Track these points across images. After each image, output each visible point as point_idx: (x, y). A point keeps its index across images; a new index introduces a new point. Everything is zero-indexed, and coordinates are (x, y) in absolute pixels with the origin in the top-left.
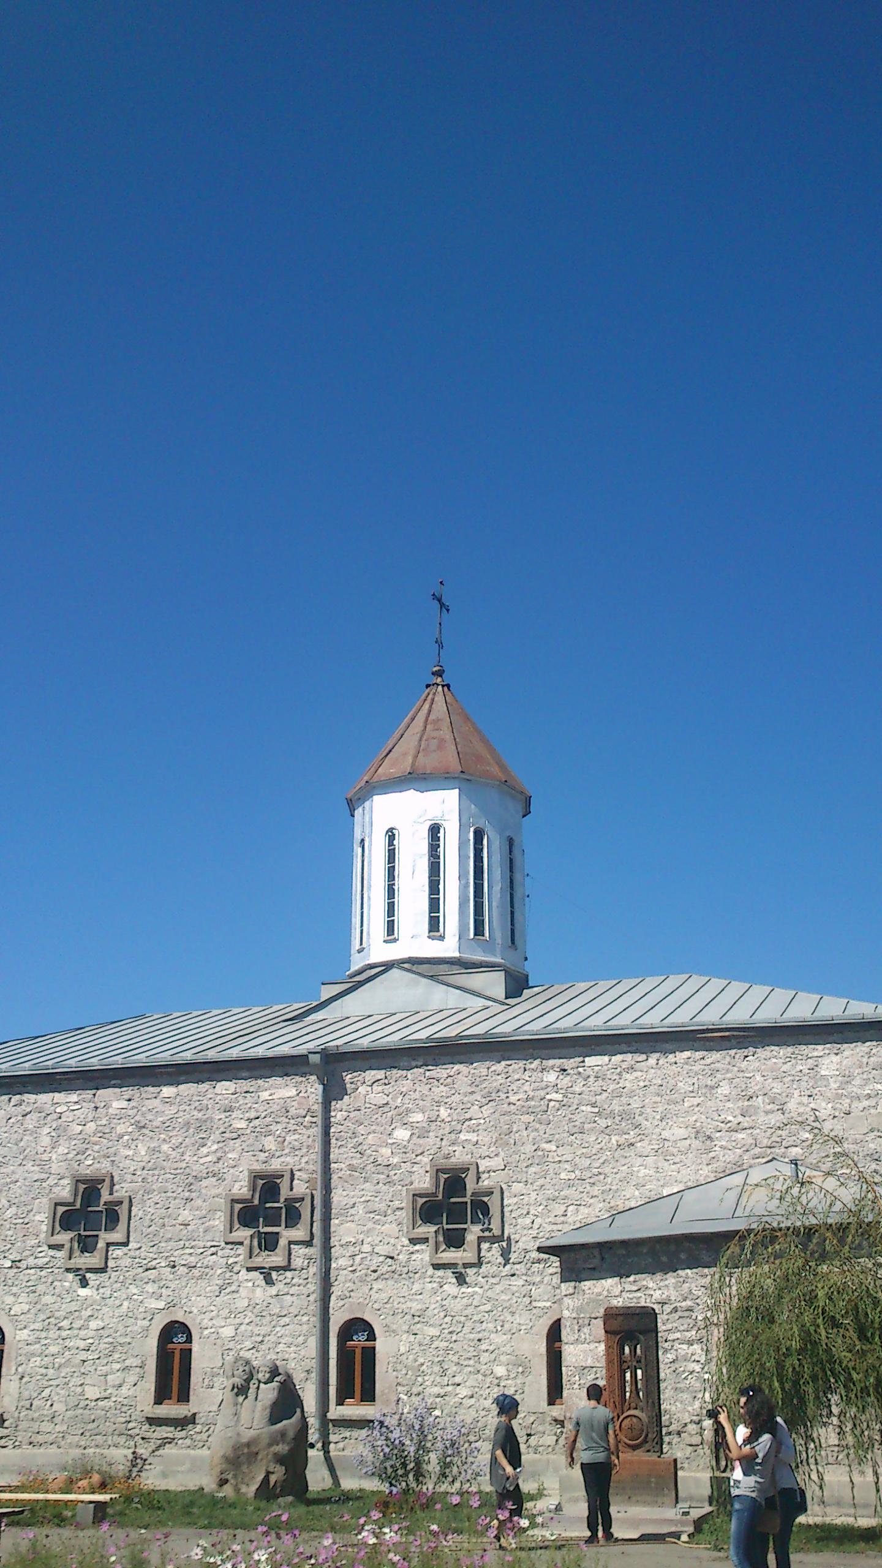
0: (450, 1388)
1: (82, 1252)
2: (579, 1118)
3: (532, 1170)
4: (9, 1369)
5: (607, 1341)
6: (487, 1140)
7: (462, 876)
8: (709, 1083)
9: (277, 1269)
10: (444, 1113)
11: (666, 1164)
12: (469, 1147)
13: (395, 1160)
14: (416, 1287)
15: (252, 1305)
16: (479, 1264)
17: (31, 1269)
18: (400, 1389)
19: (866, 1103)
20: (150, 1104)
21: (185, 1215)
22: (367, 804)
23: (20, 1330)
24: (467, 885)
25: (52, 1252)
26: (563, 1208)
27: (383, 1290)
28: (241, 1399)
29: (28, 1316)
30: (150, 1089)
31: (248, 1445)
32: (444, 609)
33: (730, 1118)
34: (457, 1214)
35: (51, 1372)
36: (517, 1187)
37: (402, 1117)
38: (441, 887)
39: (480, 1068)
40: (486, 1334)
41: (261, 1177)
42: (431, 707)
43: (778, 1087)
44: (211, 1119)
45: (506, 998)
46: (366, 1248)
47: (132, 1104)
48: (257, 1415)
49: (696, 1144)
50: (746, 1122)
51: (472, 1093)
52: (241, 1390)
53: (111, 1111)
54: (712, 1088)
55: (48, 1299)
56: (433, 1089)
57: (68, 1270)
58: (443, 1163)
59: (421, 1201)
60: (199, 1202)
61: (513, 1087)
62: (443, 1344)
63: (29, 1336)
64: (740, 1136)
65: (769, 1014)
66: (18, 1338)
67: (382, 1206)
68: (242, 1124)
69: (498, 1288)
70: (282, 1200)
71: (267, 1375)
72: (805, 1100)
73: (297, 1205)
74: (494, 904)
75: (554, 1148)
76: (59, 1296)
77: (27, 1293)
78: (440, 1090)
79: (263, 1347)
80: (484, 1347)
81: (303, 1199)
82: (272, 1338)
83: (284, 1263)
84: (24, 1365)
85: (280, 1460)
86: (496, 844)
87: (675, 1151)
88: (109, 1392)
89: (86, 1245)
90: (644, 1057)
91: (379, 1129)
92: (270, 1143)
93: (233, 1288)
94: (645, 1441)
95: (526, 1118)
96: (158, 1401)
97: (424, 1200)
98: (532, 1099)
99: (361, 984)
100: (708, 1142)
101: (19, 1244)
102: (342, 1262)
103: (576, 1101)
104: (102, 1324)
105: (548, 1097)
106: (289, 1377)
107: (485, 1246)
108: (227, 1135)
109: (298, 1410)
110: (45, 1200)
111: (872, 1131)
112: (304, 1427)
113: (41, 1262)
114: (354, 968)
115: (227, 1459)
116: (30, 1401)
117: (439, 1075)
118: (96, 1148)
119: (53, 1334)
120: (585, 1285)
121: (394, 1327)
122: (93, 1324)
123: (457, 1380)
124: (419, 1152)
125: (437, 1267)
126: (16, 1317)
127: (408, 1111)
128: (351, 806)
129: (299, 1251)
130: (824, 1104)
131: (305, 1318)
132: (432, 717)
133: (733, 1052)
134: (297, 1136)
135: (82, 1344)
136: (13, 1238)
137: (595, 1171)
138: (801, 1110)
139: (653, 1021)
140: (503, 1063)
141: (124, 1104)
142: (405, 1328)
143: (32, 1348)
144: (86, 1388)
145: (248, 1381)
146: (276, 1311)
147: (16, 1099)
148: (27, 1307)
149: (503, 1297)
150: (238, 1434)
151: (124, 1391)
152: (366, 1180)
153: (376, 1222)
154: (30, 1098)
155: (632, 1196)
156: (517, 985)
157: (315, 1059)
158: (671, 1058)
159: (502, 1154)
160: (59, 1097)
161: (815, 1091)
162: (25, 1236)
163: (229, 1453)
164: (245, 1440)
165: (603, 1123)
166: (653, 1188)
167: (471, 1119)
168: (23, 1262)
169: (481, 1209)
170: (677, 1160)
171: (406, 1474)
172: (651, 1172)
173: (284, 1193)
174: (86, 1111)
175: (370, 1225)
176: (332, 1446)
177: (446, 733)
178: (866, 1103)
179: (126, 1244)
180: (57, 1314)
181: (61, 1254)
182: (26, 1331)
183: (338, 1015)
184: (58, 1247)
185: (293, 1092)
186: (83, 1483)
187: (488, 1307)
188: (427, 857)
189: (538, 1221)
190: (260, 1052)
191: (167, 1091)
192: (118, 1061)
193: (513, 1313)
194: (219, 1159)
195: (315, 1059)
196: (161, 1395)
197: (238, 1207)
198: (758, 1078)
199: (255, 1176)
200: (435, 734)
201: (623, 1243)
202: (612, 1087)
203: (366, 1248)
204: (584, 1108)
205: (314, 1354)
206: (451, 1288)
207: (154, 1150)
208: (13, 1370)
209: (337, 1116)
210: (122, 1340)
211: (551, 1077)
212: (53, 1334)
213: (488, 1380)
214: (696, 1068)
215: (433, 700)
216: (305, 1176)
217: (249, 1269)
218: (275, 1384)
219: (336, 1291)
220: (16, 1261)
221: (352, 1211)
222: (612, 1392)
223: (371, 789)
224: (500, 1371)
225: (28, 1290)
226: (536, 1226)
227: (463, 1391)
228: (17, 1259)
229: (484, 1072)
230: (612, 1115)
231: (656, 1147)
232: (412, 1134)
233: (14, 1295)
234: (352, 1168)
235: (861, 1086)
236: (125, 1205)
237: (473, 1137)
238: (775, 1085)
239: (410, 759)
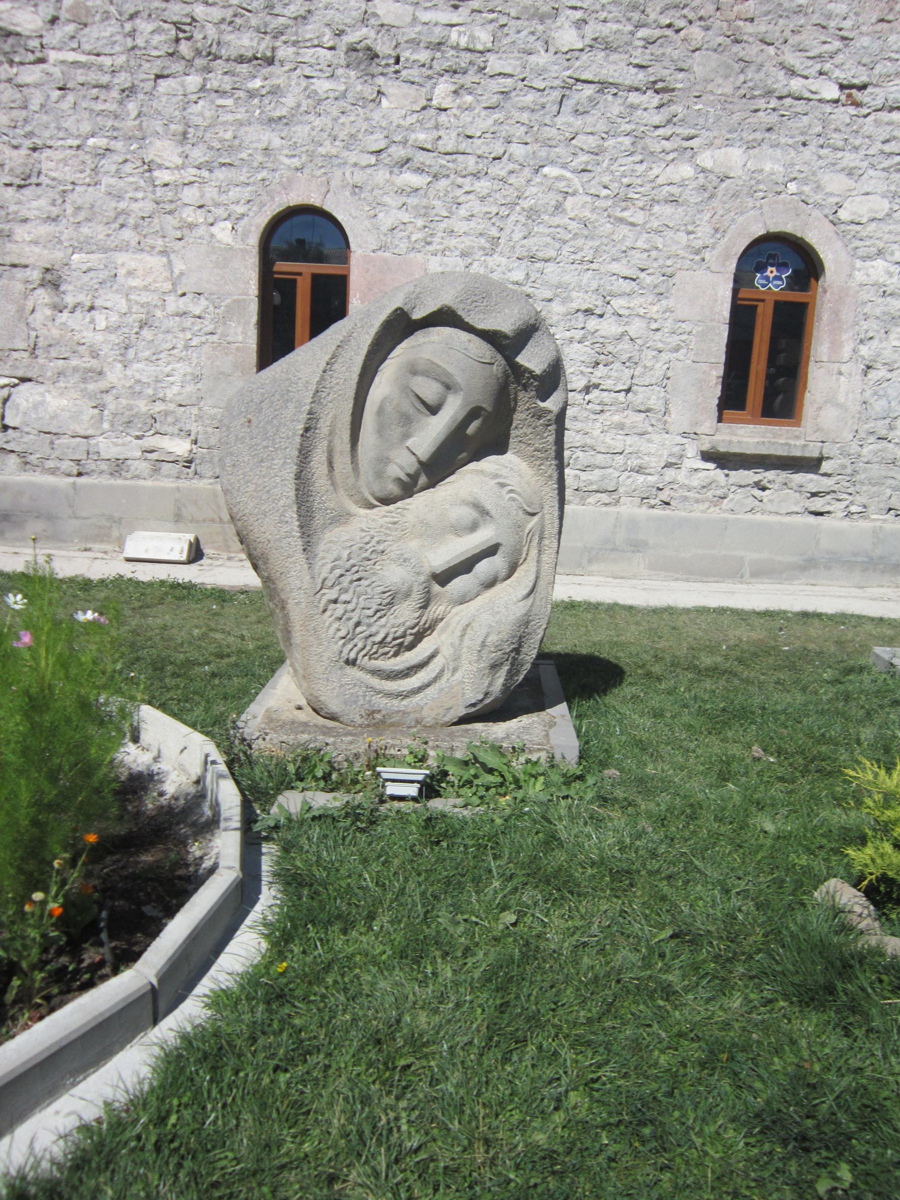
4: (836, 346)
17: (891, 109)
23: (864, 259)
29: (887, 228)
63: (890, 274)
66: (859, 277)
77: (884, 170)
84: (875, 343)
101: (865, 41)
116: (887, 421)
126: (858, 228)
136: (847, 24)
148: (884, 206)
162: (882, 20)
168: (870, 89)
182: (880, 263)
208: (846, 352)
220: (851, 87)
225: (886, 164)
228: (856, 81)
233: (850, 173)
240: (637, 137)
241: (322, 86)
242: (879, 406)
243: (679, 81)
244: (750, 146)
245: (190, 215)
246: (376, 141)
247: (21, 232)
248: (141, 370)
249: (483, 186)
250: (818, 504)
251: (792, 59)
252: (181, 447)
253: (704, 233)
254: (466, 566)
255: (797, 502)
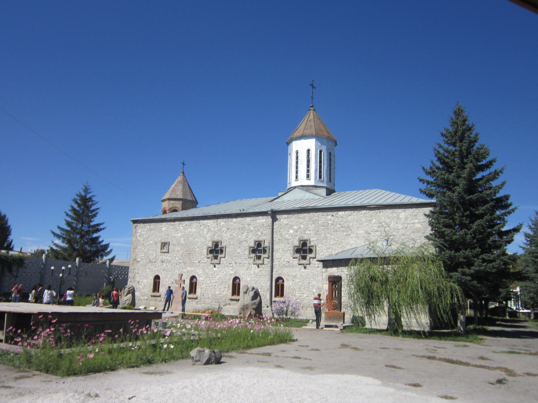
0: (302, 294)
1: (214, 259)
2: (336, 228)
3: (324, 241)
4: (198, 286)
5: (329, 283)
6: (313, 233)
7: (316, 163)
8: (370, 219)
9: (261, 264)
10: (302, 226)
11: (358, 240)
12: (308, 235)
13: (290, 238)
14: (294, 269)
15: (255, 273)
16: (310, 264)
18: (290, 294)
19: (411, 225)
20: (230, 223)
21: (239, 251)
22: (291, 144)
24: (317, 166)
25: (207, 259)
26: (331, 251)
27: (286, 270)
28: (245, 295)
30: (230, 219)
31: (246, 305)
32: (314, 88)
33: (375, 228)
34: (305, 251)
35: (208, 288)
36: (320, 245)
37: (291, 227)
38: (310, 166)
39: (311, 214)
40: (311, 281)
41: (257, 242)
42: (309, 116)
43: (388, 221)
44: (245, 227)
45: (326, 195)
46: (282, 260)
47: (226, 223)
48: (249, 298)
49: (366, 235)
50: (379, 229)
51: (309, 221)
52: (246, 293)
53: (221, 225)
54: (371, 220)
55: (207, 271)
56: (300, 220)
57: (211, 264)
58: (301, 239)
59: (296, 248)
60: (242, 247)
61: (320, 220)
62: (300, 284)
64: (378, 233)
65: (398, 201)
67: (287, 249)
68: (252, 228)
69: (314, 270)
70: (262, 247)
71: (251, 290)
72: (395, 224)
73: (266, 249)
74: (324, 171)
75: (329, 235)
76: (209, 270)
78: (301, 220)
79: (257, 283)
80: (310, 284)
81: (267, 247)
82: (259, 281)
83: (262, 263)
85: (254, 309)
86: (326, 154)
87: (360, 237)
88: (221, 292)
89: (216, 258)
90: (353, 212)
91: (286, 230)
92: (259, 233)
93: (250, 269)
94: (337, 308)
95: (322, 228)
96: (233, 295)
97: (297, 248)
98: (324, 223)
99: (287, 192)
100: (369, 235)
102: (276, 263)
103: (335, 224)
104: (219, 277)
105: (328, 222)
106: (258, 290)
107: (311, 260)
108: (249, 231)
109: (259, 298)
110: (206, 247)
111: (413, 232)
112: (260, 303)
113: (205, 261)
114: (288, 188)
115: (241, 308)
117: (301, 217)
118: (218, 234)
119: (208, 279)
120: (329, 269)
121: (289, 279)
122: (217, 277)
123: (304, 292)
124: (296, 236)
125: (299, 264)
127: (293, 226)
128: (288, 143)
129: (266, 260)
130: (400, 225)
131: (267, 277)
132: (309, 119)
133: (377, 211)
134: (266, 232)
135: (215, 281)
137: (340, 241)
138: (394, 227)
139: (358, 203)
140: (318, 213)
141: (224, 223)
142: (291, 279)
143: (203, 282)
144: (216, 292)
145: (247, 290)
146: (260, 274)
147: (199, 221)
149: (316, 272)
150: (244, 303)
151: (225, 292)
152: (283, 243)
153: (285, 253)
154: (202, 221)
155: (349, 247)
156: (330, 192)
157: (270, 212)
158: (360, 212)
159: (316, 237)
160: (208, 221)
161: (398, 222)
163: (242, 307)
164: (245, 304)
165: (342, 229)
166: (354, 246)
167: (309, 228)
169: (311, 251)
170: (361, 239)
171: (283, 314)
172: (354, 242)
173: (263, 246)
174: (215, 225)
175: (283, 254)
176: (273, 307)
177: (312, 124)
178: (411, 225)
179: (225, 257)
180: (209, 274)
181: (210, 260)
182: (202, 278)
183: (282, 200)
184: (209, 258)
185: (265, 220)
186: (207, 312)
187: (312, 275)
188: (306, 158)
189: (325, 254)
190: (257, 210)
191: (234, 220)
192: (223, 213)
193: (318, 277)
194: (247, 237)
195: (270, 212)
196: (233, 293)
197: (251, 249)
198: (383, 218)
199: (255, 242)
200: (310, 124)
201: (339, 260)
202: (345, 220)
203: (282, 260)
204: (337, 225)
205: (269, 285)
206: (303, 270)
207: (231, 235)
209: (275, 227)
210: (224, 281)
211: (329, 217)
212: (208, 279)
213: (311, 293)
214: (367, 215)
215: (310, 114)
216: (267, 241)
217: (254, 264)
218: (253, 292)
219: (275, 270)
221: (279, 250)
222: (329, 296)
223: (292, 140)
224: (314, 291)
226: (324, 255)
227: (305, 295)
229: (312, 216)
230: (344, 227)
231: (355, 235)
232: (294, 231)
234: (279, 240)
235: (411, 221)
236: (225, 248)
237: (309, 232)
238: (387, 220)
239: (302, 131)
240: (182, 267)
241: (159, 264)
242: (202, 292)
243: (186, 262)
244: (191, 267)
245: (149, 276)
246: (163, 269)
247: (137, 278)
248: (144, 290)
249: (170, 272)
250: (197, 303)
251: (194, 259)
252: (146, 298)
253: (187, 276)
254: (127, 300)
255: (195, 303)
